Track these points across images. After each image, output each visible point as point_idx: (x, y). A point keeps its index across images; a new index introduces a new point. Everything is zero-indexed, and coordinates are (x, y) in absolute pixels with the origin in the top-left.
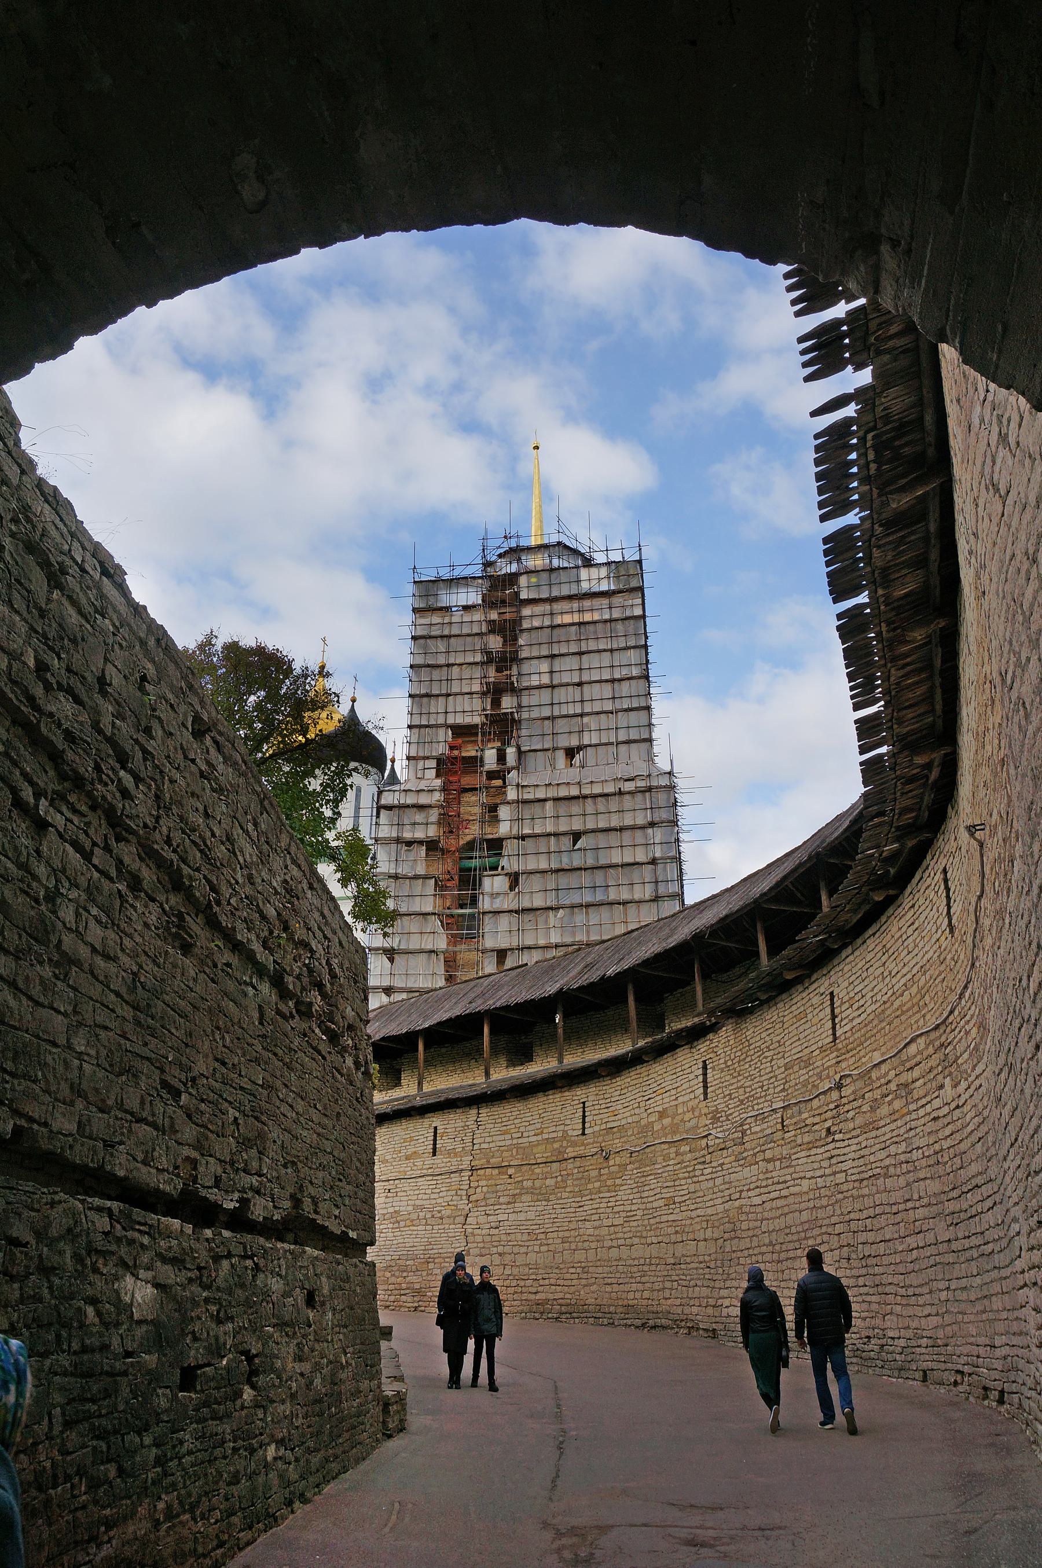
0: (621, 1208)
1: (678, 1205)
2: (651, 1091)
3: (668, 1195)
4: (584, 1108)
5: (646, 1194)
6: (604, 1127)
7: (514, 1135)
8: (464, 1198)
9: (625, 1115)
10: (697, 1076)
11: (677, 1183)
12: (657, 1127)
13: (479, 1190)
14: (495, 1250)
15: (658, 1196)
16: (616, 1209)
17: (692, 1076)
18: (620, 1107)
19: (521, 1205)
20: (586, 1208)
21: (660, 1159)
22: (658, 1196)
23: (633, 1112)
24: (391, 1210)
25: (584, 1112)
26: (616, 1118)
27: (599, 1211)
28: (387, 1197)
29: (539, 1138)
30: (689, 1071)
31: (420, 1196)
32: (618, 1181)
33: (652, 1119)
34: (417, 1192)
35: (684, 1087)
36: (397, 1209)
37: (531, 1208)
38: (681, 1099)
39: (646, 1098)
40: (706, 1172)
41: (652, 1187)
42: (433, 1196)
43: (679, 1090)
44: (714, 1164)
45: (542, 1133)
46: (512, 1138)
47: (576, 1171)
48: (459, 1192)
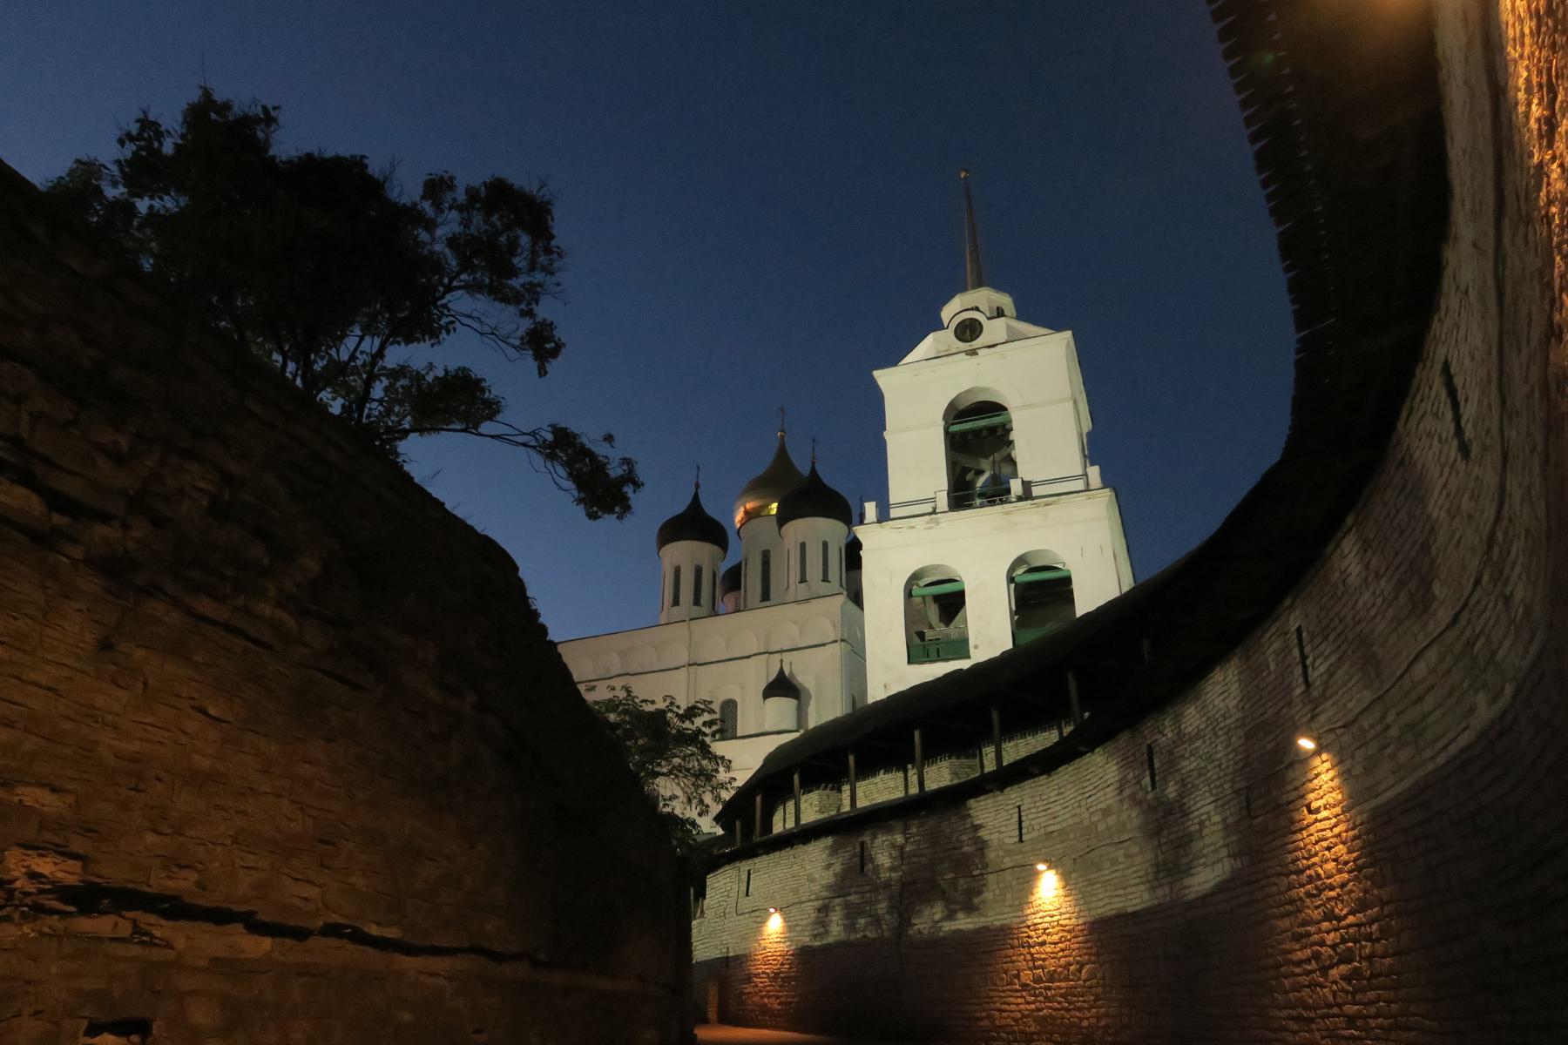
2: (1091, 787)
5: (1093, 905)
6: (1043, 831)
9: (1065, 817)
11: (1128, 890)
12: (1101, 827)
18: (1058, 808)
21: (1107, 864)
23: (1073, 812)
25: (1020, 817)
26: (1056, 821)
33: (1095, 819)
39: (1087, 795)
41: (1100, 896)
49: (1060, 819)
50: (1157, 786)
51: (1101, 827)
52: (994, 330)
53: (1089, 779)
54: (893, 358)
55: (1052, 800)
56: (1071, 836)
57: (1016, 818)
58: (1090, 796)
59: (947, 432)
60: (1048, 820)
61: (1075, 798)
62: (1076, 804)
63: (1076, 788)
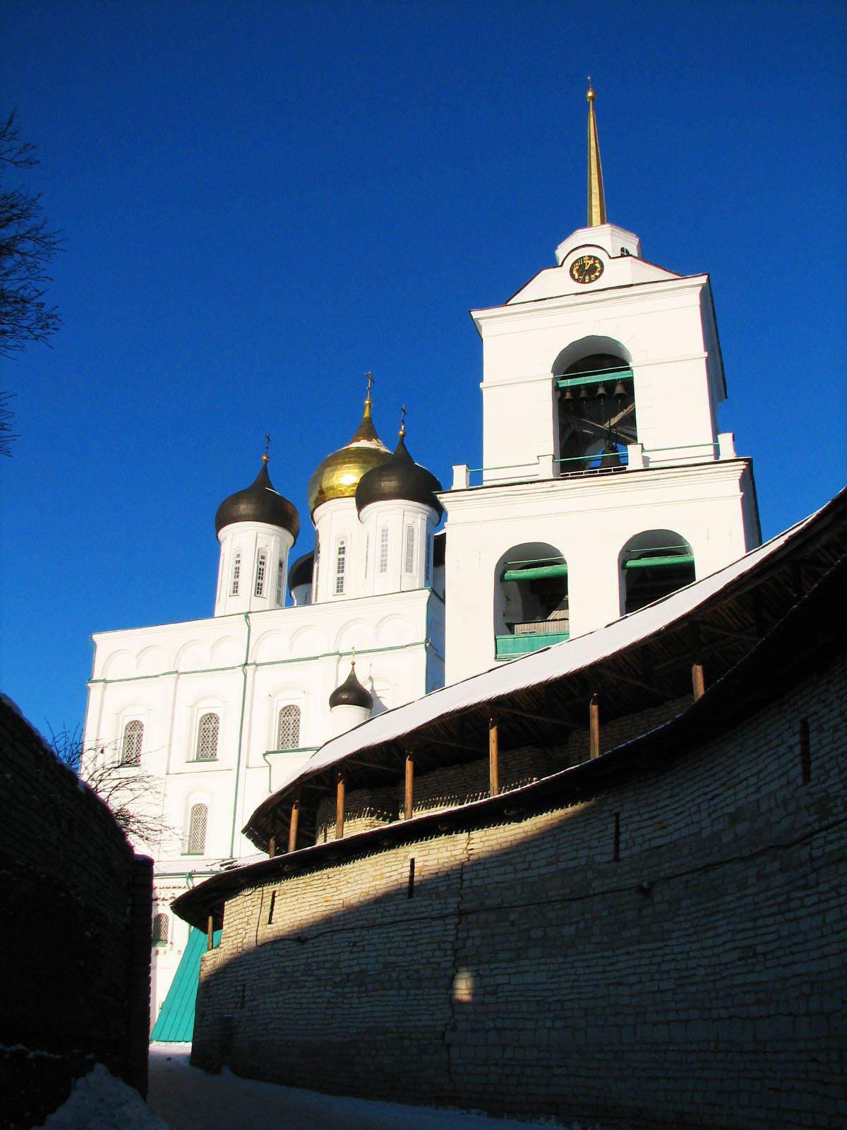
0: (673, 965)
1: (761, 958)
2: (717, 784)
3: (745, 943)
4: (617, 822)
5: (709, 943)
6: (646, 846)
7: (520, 866)
8: (449, 952)
10: (791, 748)
11: (760, 922)
12: (727, 837)
13: (469, 943)
14: (491, 1025)
15: (727, 946)
16: (665, 967)
17: (782, 750)
18: (670, 814)
19: (527, 962)
20: (620, 965)
22: (727, 946)
23: (689, 820)
24: (356, 969)
25: (617, 827)
27: (640, 970)
28: (351, 952)
29: (553, 868)
30: (778, 741)
31: (392, 951)
32: (668, 925)
34: (389, 945)
35: (772, 767)
36: (364, 967)
37: (542, 967)
38: (765, 790)
39: (709, 796)
40: (808, 901)
41: (719, 931)
42: (409, 950)
43: (761, 776)
44: (823, 887)
45: (558, 861)
46: (516, 871)
47: (605, 913)
48: (442, 946)
49: (670, 829)
50: (813, 775)
51: (727, 837)
52: (617, 271)
53: (715, 775)
54: (502, 294)
55: (660, 805)
56: (685, 851)
57: (612, 829)
58: (715, 797)
59: (556, 388)
60: (654, 831)
61: (693, 800)
62: (695, 809)
63: (696, 787)
